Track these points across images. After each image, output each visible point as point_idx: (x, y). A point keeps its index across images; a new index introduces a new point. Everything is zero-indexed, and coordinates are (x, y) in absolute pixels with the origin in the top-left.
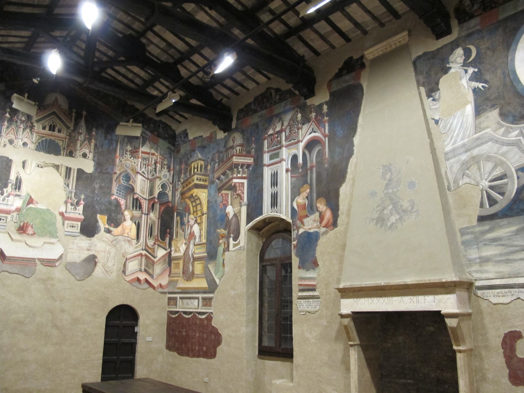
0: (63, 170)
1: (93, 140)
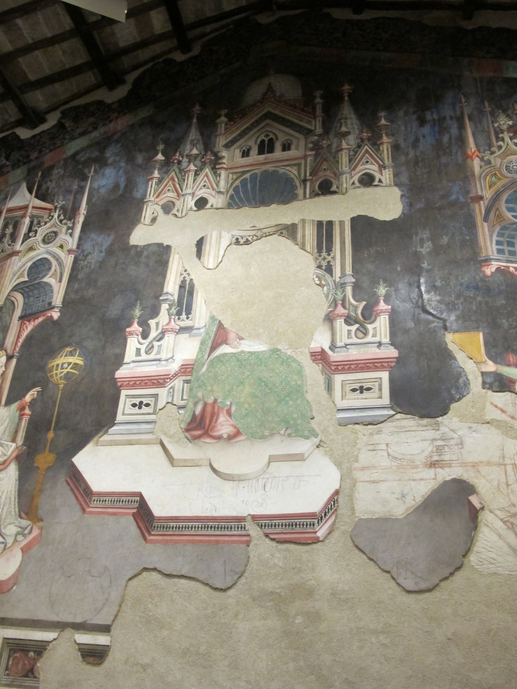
0: (310, 234)
1: (385, 139)
